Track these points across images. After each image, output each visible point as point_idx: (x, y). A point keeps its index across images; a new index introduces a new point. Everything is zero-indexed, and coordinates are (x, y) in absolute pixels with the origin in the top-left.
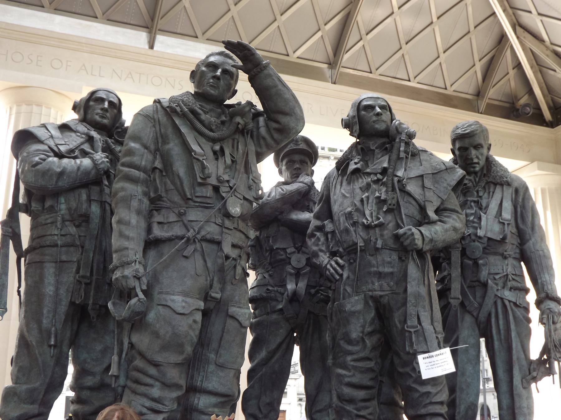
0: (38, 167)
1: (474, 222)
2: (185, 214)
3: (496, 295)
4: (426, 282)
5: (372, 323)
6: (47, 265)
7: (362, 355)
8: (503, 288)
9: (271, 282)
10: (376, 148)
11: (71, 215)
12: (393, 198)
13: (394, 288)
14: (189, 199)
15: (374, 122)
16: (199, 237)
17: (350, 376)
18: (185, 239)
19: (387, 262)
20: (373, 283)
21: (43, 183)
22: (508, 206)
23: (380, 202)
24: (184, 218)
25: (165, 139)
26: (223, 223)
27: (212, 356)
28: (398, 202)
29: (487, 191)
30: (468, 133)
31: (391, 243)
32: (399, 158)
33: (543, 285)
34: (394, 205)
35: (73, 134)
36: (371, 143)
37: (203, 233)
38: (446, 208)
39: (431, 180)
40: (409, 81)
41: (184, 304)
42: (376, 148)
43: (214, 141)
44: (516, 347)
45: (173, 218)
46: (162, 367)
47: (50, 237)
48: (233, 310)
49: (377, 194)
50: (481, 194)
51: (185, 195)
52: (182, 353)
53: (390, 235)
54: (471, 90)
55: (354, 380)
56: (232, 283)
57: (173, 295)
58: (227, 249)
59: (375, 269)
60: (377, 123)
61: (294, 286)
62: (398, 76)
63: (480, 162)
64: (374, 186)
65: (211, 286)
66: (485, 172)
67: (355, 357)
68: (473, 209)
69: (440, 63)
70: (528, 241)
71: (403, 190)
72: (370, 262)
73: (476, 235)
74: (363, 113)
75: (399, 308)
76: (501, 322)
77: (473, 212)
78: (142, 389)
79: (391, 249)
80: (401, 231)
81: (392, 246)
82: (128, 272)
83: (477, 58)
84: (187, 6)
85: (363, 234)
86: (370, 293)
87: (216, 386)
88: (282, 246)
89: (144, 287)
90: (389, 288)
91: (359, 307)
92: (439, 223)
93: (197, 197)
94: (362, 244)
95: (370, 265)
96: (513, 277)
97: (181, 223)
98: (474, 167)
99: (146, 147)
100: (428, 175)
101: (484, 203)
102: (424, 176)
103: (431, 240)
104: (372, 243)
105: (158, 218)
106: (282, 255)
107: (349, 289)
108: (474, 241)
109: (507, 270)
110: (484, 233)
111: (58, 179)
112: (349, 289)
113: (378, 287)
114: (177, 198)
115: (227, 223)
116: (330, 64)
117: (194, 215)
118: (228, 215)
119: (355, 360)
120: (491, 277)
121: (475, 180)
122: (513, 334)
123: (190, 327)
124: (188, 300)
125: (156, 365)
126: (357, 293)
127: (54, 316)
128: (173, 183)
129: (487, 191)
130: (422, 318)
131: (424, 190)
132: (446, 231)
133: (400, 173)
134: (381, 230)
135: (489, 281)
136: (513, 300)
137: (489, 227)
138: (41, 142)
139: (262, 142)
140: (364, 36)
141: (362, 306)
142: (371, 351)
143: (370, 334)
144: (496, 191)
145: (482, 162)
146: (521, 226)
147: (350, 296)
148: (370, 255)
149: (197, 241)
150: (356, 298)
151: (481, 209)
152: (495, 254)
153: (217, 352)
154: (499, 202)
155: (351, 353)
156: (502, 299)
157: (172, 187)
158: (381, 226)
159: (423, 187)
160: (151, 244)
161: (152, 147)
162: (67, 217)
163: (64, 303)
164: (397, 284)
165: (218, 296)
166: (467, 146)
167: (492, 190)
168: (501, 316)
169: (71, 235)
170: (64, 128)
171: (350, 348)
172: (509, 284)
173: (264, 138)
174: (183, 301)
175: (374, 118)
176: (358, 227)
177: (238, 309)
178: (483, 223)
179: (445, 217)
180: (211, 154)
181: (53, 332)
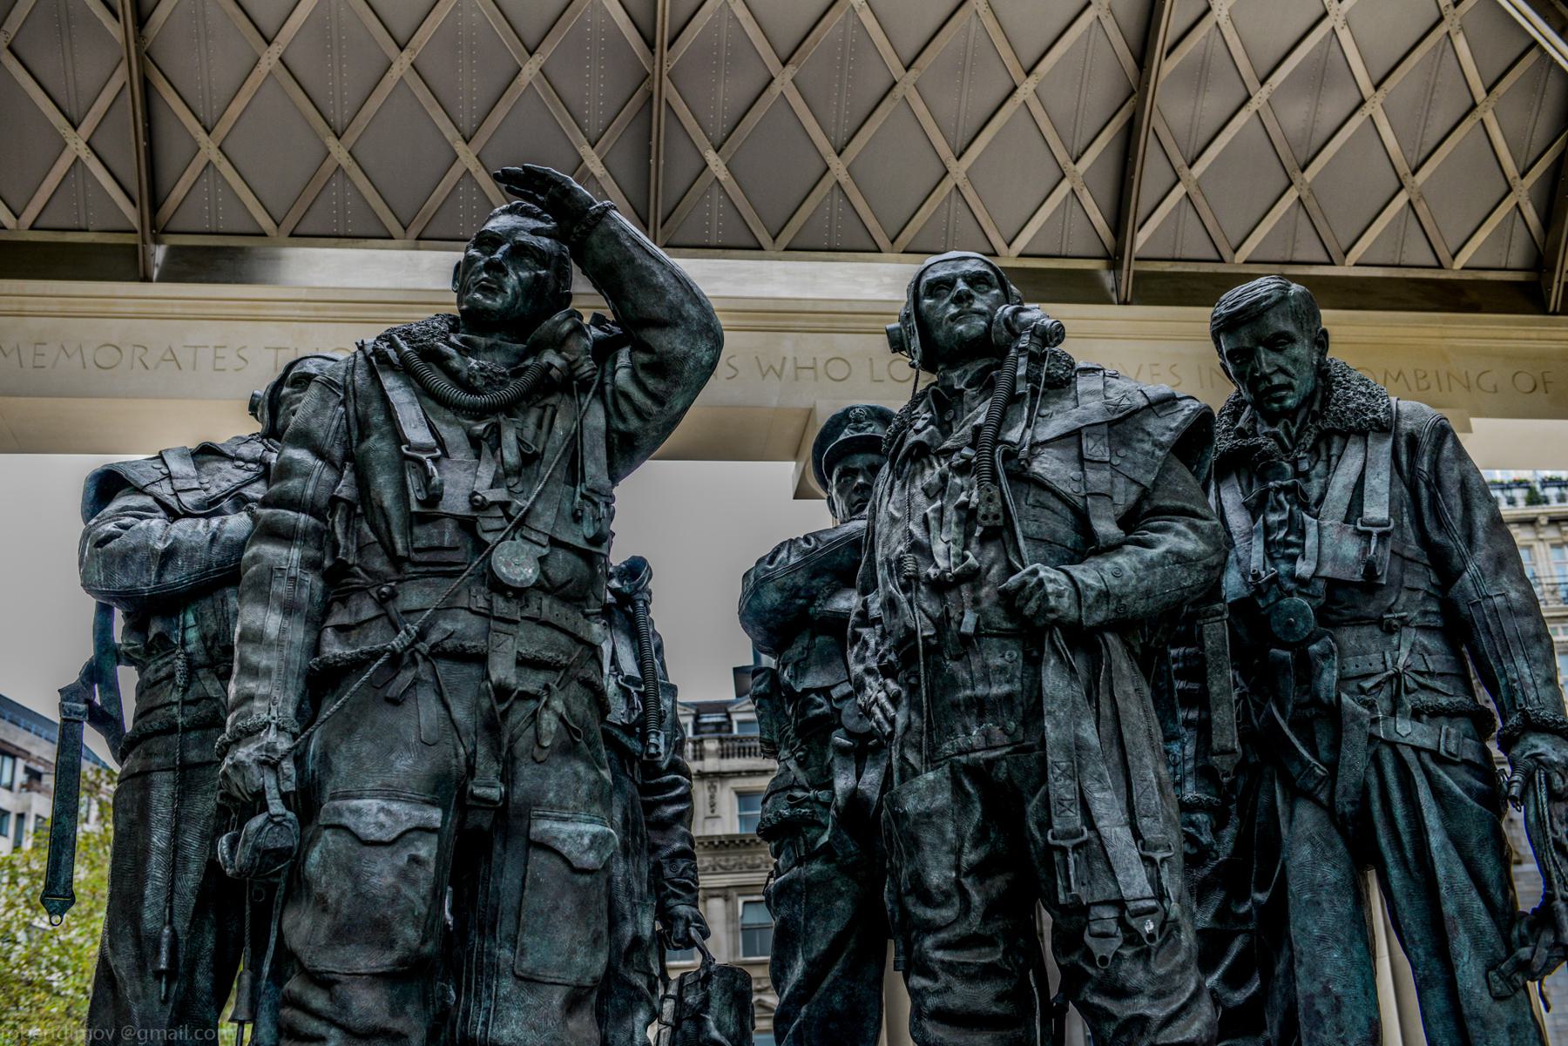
0: (111, 545)
1: (1289, 545)
2: (393, 596)
3: (1372, 738)
4: (1106, 710)
5: (981, 837)
6: (157, 777)
7: (960, 930)
8: (1393, 714)
9: (802, 778)
10: (969, 385)
11: (208, 650)
12: (990, 500)
15: (953, 318)
16: (424, 647)
17: (937, 993)
18: (387, 655)
20: (969, 734)
21: (127, 582)
22: (1380, 482)
23: (968, 515)
24: (391, 606)
25: (363, 427)
26: (491, 608)
27: (505, 954)
29: (1324, 457)
30: (1240, 311)
31: (997, 618)
32: (1014, 399)
33: (1511, 691)
34: (996, 517)
35: (227, 466)
36: (955, 375)
37: (434, 637)
38: (1159, 507)
39: (1106, 440)
41: (382, 817)
42: (969, 385)
43: (478, 413)
44: (1449, 877)
45: (368, 610)
46: (337, 987)
47: (160, 712)
48: (544, 827)
49: (963, 497)
50: (1304, 466)
51: (394, 549)
52: (390, 944)
53: (995, 597)
54: (1517, 257)
55: (954, 1001)
56: (534, 759)
57: (360, 797)
58: (502, 670)
59: (968, 692)
60: (960, 322)
61: (851, 781)
62: (1298, 257)
63: (1296, 383)
64: (958, 480)
65: (471, 770)
66: (1316, 407)
67: (943, 935)
68: (1283, 509)
69: (1410, 202)
70: (1460, 573)
71: (1022, 478)
72: (953, 678)
73: (1291, 576)
74: (928, 301)
76: (1399, 811)
77: (1285, 516)
79: (1003, 635)
80: (1013, 580)
81: (1005, 625)
82: (244, 753)
83: (1511, 168)
84: (722, 178)
87: (519, 1033)
88: (819, 684)
89: (289, 786)
90: (1006, 740)
91: (943, 798)
92: (1130, 548)
93: (418, 550)
95: (953, 683)
96: (1421, 680)
97: (385, 620)
98: (1282, 399)
99: (319, 453)
100: (1095, 429)
101: (1314, 490)
102: (1084, 432)
103: (1105, 595)
104: (953, 626)
106: (821, 706)
107: (912, 757)
108: (1290, 594)
109: (1395, 662)
110: (1313, 567)
111: (162, 567)
112: (912, 757)
113: (973, 738)
114: (379, 563)
115: (500, 605)
116: (1107, 257)
117: (414, 597)
118: (498, 586)
119: (940, 946)
120: (1353, 686)
121: (1288, 433)
122: (1436, 839)
123: (403, 875)
124: (395, 807)
125: (325, 982)
126: (932, 761)
127: (170, 899)
128: (374, 528)
129: (1324, 457)
130: (1098, 809)
131: (1082, 470)
132: (1151, 565)
133: (1013, 435)
134: (975, 589)
135: (1345, 698)
136: (1428, 743)
137: (1326, 550)
138: (140, 491)
139: (622, 402)
141: (947, 795)
142: (986, 918)
143: (980, 871)
144: (1347, 451)
145: (1304, 382)
146: (1436, 537)
147: (916, 773)
148: (952, 659)
149: (419, 657)
150: (931, 776)
151: (1305, 507)
152: (1358, 621)
153: (514, 942)
154: (1354, 479)
155: (930, 928)
156: (1393, 745)
157: (373, 538)
158: (973, 577)
159: (1082, 460)
160: (320, 682)
161: (337, 452)
162: (200, 658)
163: (193, 867)
165: (495, 793)
167: (1334, 451)
168: (1396, 795)
169: (209, 698)
170: (206, 453)
171: (930, 913)
172: (1408, 702)
173: (626, 396)
174: (382, 809)
175: (953, 310)
176: (918, 589)
177: (556, 825)
178: (1311, 542)
179: (1154, 530)
180: (466, 445)
181: (165, 940)
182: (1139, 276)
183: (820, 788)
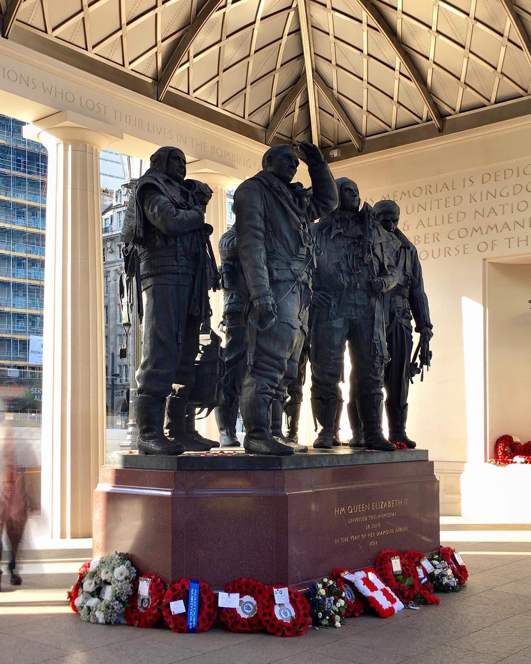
8: (402, 317)
13: (364, 315)
14: (294, 255)
19: (359, 298)
28: (372, 260)
40: (217, 106)
85: (347, 278)
94: (347, 285)
97: (290, 271)
105: (274, 265)
107: (334, 313)
112: (334, 313)
126: (340, 316)
140: (86, 8)
147: (335, 319)
156: (401, 325)
166: (389, 219)
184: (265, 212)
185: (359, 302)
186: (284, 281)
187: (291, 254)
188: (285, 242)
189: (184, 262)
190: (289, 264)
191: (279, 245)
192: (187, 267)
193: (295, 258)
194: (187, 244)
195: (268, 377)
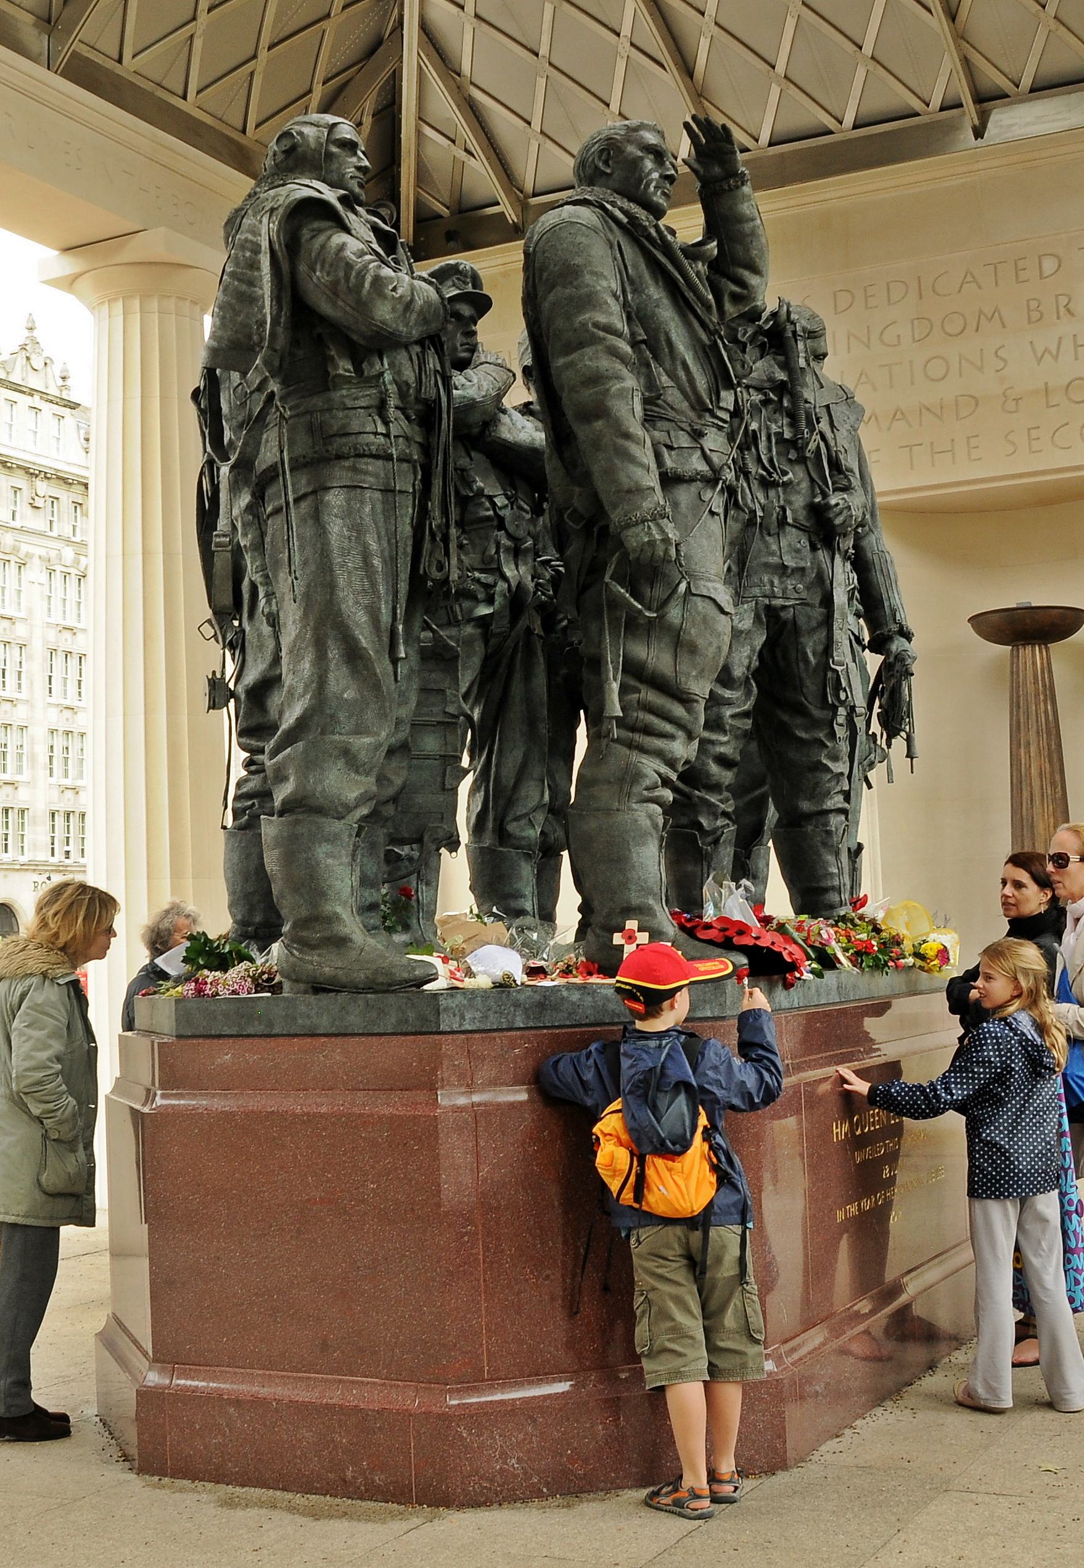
13: (804, 595)
33: (894, 613)
75: (813, 630)
78: (659, 743)
83: (320, 75)
85: (760, 495)
86: (767, 601)
97: (699, 453)
106: (488, 510)
128: (672, 375)
155: (729, 703)
164: (808, 588)
182: (75, 55)
183: (482, 571)
184: (624, 291)
185: (790, 562)
186: (692, 480)
187: (699, 407)
188: (682, 374)
189: (399, 425)
190: (697, 435)
191: (665, 380)
192: (407, 438)
193: (708, 418)
194: (409, 375)
195: (659, 754)
